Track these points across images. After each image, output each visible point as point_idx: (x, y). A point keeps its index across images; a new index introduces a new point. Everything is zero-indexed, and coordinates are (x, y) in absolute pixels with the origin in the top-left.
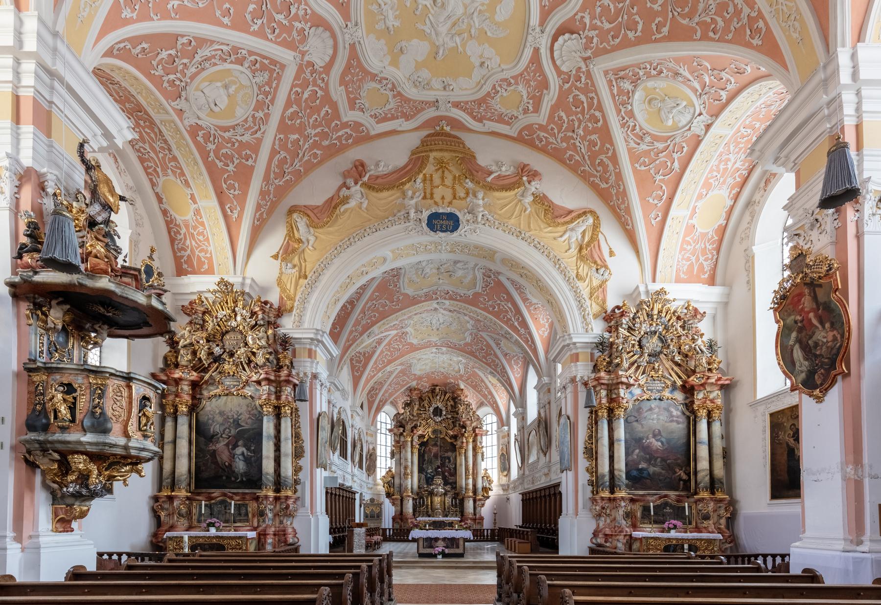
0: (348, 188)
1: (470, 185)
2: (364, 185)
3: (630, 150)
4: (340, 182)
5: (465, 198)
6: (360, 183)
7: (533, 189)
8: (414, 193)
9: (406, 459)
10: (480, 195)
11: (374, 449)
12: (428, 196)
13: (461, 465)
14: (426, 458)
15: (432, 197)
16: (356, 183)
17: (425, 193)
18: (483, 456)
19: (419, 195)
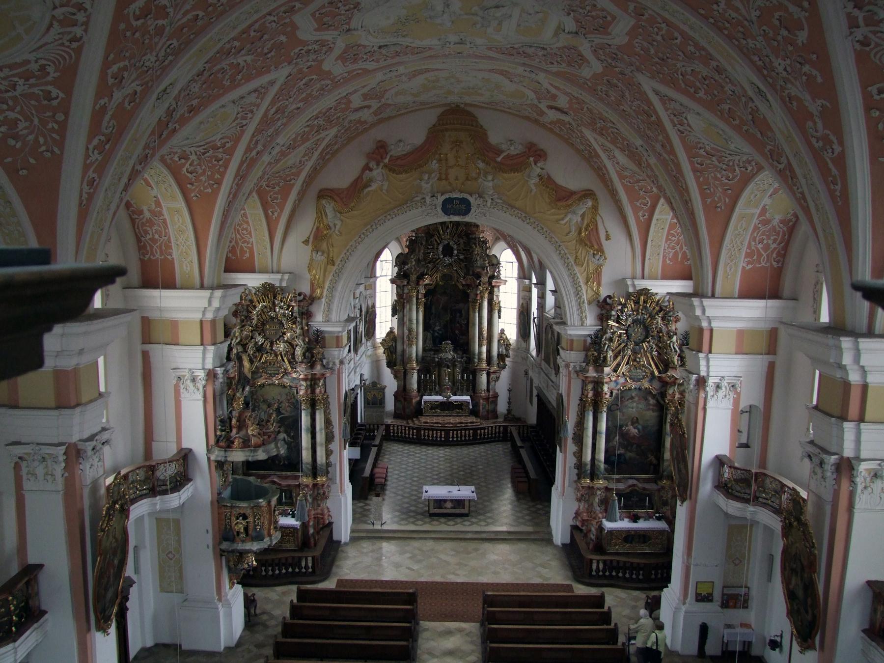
0: (371, 170)
1: (481, 165)
2: (386, 166)
3: (617, 172)
4: (362, 162)
5: (476, 179)
6: (382, 164)
7: (539, 170)
8: (430, 173)
9: (410, 320)
10: (490, 178)
11: (374, 306)
12: (444, 176)
13: (474, 324)
14: (433, 311)
15: (447, 179)
16: (378, 165)
17: (440, 174)
18: (500, 311)
19: (435, 176)
